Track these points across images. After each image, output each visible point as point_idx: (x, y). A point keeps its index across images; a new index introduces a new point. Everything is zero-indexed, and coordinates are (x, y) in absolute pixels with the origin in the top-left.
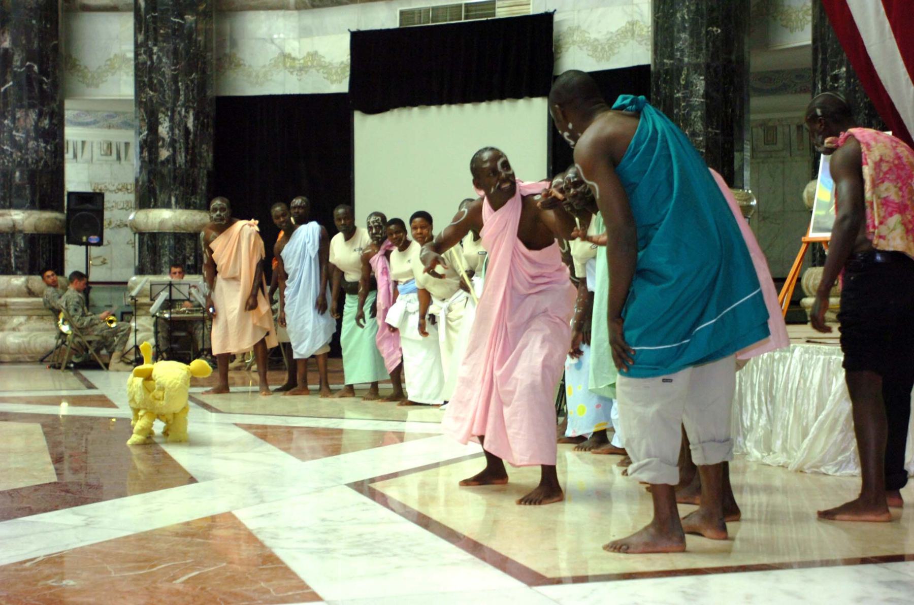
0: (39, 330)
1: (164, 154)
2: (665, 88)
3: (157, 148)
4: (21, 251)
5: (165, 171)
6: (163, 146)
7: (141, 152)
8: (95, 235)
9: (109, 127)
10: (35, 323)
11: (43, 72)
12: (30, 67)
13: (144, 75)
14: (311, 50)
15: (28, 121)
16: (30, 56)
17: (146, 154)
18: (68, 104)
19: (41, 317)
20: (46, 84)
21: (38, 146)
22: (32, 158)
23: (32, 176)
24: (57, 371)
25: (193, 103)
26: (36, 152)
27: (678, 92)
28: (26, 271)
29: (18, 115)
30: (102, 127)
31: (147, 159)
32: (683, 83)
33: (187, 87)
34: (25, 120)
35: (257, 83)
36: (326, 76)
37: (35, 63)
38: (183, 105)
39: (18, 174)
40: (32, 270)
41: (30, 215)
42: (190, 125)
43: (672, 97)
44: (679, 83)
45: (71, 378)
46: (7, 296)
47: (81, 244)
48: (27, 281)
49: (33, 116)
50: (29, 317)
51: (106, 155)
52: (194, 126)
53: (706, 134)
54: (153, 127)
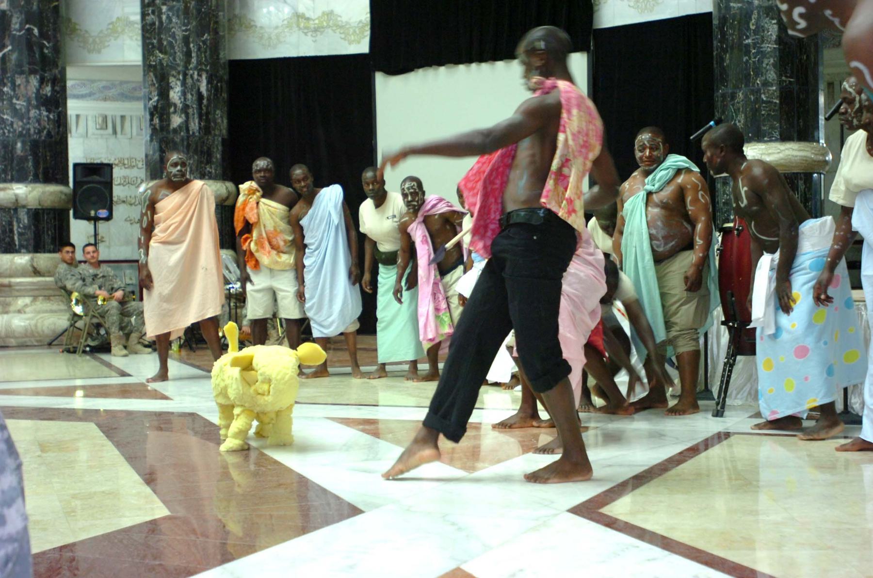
0: (46, 312)
1: (177, 120)
2: (733, 34)
3: (168, 114)
4: (25, 228)
5: (177, 139)
6: (175, 112)
7: (151, 120)
8: (103, 208)
9: (105, 99)
10: (41, 305)
12: (29, 31)
13: (152, 35)
14: (326, 9)
15: (29, 88)
16: (29, 18)
17: (156, 121)
19: (48, 298)
20: (47, 48)
21: (40, 115)
22: (35, 128)
23: (35, 146)
24: (72, 356)
25: (206, 66)
26: (38, 121)
27: (748, 38)
28: (31, 248)
29: (18, 82)
30: (97, 99)
31: (157, 126)
32: (753, 27)
33: (199, 49)
34: (26, 87)
35: (269, 46)
36: (343, 36)
37: (35, 26)
38: (195, 68)
39: (19, 145)
40: (38, 248)
41: (33, 189)
42: (203, 89)
43: (741, 44)
44: (748, 29)
45: (86, 363)
46: (11, 276)
47: (88, 218)
48: (32, 259)
49: (34, 81)
50: (35, 298)
51: (101, 129)
52: (207, 90)
53: (780, 82)
54: (164, 93)
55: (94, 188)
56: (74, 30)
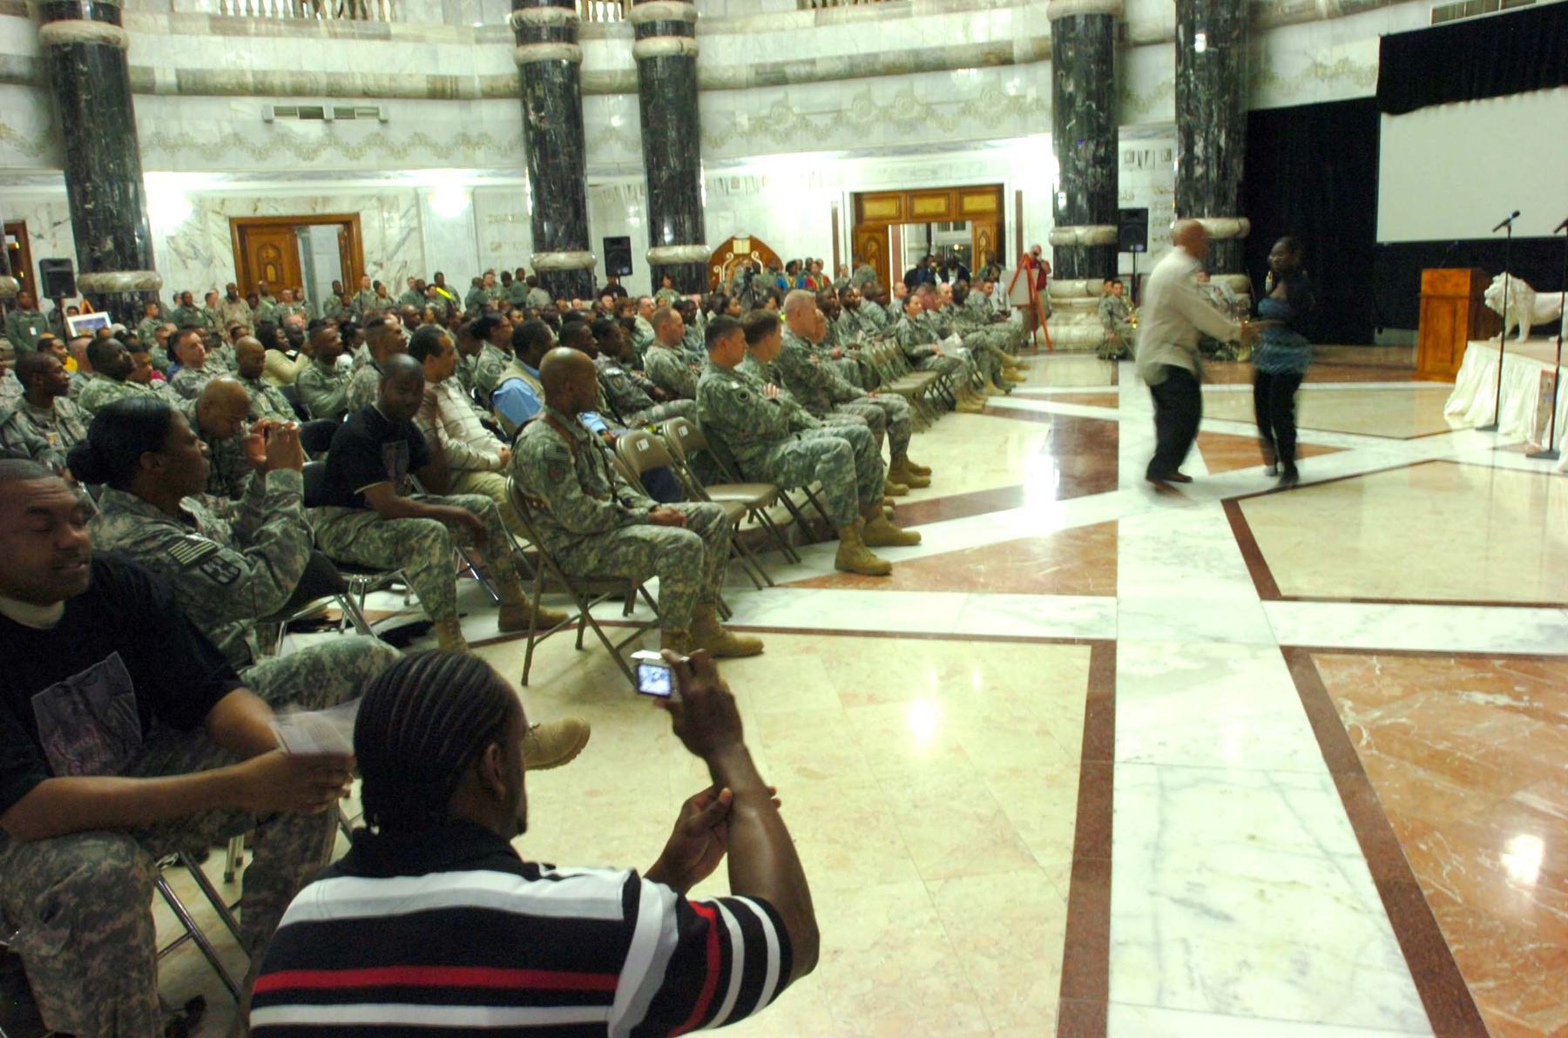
1: (1199, 170)
5: (1199, 186)
11: (1100, 108)
13: (1185, 99)
18: (1123, 132)
23: (1091, 199)
33: (1220, 109)
40: (1091, 276)
42: (1222, 143)
49: (1092, 146)
55: (1132, 229)
56: (1128, 96)
